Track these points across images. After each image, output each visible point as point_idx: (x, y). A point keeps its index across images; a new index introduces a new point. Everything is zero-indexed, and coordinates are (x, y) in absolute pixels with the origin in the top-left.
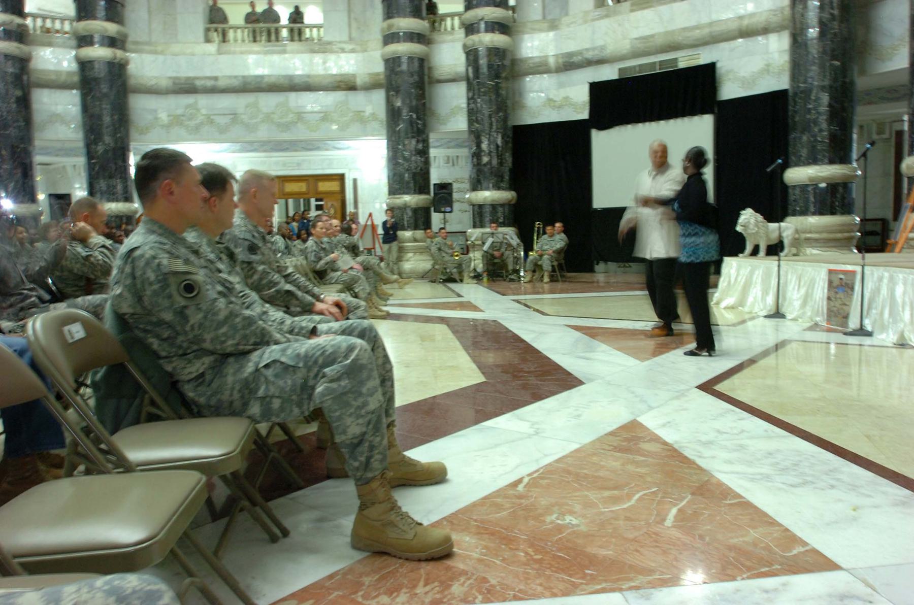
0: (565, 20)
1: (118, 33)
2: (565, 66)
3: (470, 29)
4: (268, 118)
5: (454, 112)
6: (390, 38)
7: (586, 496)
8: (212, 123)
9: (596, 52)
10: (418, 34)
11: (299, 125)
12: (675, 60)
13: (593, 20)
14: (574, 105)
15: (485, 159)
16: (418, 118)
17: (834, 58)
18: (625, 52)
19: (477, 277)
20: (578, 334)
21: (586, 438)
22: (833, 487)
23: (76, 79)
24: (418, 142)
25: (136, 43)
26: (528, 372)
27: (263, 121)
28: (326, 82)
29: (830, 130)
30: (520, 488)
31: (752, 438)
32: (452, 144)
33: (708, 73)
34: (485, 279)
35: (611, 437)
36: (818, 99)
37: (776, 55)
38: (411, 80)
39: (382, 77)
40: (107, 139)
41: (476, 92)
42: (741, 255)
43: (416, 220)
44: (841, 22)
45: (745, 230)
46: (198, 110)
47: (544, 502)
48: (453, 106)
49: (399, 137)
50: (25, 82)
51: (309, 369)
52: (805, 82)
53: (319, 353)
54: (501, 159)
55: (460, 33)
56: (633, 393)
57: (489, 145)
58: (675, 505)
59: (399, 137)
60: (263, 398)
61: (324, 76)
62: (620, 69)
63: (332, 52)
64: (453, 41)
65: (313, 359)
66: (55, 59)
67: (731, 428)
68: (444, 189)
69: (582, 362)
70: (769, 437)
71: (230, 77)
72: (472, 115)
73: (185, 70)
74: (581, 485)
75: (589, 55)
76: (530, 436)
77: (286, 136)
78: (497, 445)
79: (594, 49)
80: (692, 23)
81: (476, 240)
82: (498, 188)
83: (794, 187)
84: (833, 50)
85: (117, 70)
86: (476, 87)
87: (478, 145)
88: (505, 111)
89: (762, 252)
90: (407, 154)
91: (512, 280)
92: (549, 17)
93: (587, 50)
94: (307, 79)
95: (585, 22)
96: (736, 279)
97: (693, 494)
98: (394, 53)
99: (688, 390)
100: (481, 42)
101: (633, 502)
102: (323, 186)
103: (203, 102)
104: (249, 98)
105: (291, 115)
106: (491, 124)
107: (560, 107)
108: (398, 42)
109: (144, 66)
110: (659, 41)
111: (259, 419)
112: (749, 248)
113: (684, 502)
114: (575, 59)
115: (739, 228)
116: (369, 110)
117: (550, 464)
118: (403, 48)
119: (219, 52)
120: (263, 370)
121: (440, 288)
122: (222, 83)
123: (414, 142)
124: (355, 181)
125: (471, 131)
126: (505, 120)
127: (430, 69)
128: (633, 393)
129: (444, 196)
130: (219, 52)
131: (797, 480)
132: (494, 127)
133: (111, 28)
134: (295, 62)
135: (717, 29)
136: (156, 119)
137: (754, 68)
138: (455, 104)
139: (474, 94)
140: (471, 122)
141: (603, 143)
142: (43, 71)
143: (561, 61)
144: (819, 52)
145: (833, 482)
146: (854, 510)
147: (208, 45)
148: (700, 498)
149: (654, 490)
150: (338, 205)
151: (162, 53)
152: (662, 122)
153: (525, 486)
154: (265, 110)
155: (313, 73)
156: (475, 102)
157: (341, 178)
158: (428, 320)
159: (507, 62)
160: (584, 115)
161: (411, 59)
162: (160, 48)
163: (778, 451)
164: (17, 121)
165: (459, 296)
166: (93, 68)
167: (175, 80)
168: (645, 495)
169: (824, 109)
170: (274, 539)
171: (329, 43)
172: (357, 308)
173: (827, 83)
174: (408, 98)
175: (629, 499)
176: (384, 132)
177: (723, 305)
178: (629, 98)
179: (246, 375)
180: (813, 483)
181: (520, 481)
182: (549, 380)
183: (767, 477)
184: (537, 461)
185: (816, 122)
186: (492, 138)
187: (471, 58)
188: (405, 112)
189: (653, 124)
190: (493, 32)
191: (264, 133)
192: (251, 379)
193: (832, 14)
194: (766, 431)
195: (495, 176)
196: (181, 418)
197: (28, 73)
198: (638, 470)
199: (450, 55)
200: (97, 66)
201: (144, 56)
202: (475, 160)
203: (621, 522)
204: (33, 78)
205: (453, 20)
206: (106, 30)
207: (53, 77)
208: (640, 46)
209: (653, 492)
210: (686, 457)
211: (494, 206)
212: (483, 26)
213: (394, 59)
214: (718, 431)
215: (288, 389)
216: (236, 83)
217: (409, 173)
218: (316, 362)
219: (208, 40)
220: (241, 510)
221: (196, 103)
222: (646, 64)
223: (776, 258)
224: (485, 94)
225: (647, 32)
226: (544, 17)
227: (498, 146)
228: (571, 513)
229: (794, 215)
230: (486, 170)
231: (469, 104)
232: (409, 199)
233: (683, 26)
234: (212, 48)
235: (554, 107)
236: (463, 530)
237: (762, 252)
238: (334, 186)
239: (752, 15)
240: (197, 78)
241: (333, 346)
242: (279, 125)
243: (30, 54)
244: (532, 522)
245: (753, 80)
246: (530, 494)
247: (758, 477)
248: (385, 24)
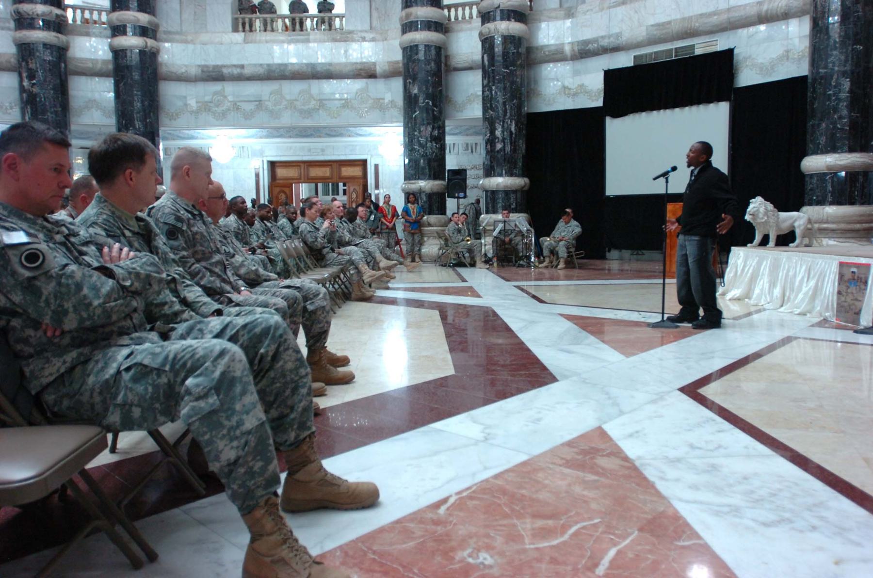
0: (581, 8)
1: (149, 22)
2: (581, 53)
3: (486, 17)
4: (291, 105)
5: (469, 101)
6: (408, 27)
7: (514, 526)
8: (238, 109)
9: (612, 39)
10: (436, 23)
11: (321, 111)
12: (692, 47)
13: (610, 7)
14: (588, 93)
15: (499, 146)
16: (434, 105)
17: (857, 42)
18: (640, 39)
19: (488, 261)
20: (568, 324)
21: (540, 447)
22: (814, 528)
23: (111, 67)
24: (433, 128)
25: (169, 33)
26: (503, 366)
27: (286, 108)
28: (346, 70)
29: (850, 117)
30: (442, 510)
31: (727, 456)
32: (471, 131)
33: (725, 60)
34: (495, 264)
35: (566, 449)
36: (838, 85)
37: (796, 41)
39: (401, 65)
41: (491, 79)
42: (749, 245)
43: (430, 207)
45: (754, 219)
46: (225, 97)
47: (462, 531)
48: (469, 91)
49: (415, 124)
50: (63, 70)
51: (177, 374)
52: (826, 67)
53: (188, 356)
54: (515, 146)
55: (477, 22)
56: (607, 394)
57: (503, 132)
58: (615, 545)
60: (123, 405)
61: (346, 64)
62: (635, 57)
63: (353, 40)
64: (471, 30)
65: (181, 362)
66: (93, 48)
67: (706, 442)
68: (459, 175)
69: (563, 356)
70: (748, 456)
71: (255, 65)
72: (488, 103)
73: (213, 58)
74: (513, 510)
75: (605, 43)
76: (477, 443)
77: (308, 122)
78: (436, 453)
79: (609, 37)
80: (711, 9)
81: (487, 225)
82: (511, 175)
83: (811, 176)
84: (856, 34)
85: (149, 58)
86: (491, 75)
87: (492, 132)
88: (520, 99)
89: (772, 243)
90: (422, 140)
91: (522, 266)
92: (566, 5)
93: (603, 37)
94: (328, 67)
95: (602, 9)
96: (743, 270)
97: (641, 530)
98: (412, 41)
99: (669, 392)
100: (496, 29)
101: (566, 537)
102: (347, 172)
103: (229, 88)
104: (273, 86)
105: (313, 102)
106: (505, 112)
107: (575, 95)
108: (417, 30)
109: (174, 54)
110: (675, 28)
111: (119, 428)
112: (758, 238)
113: (627, 541)
114: (591, 47)
115: (747, 217)
116: (388, 97)
117: (487, 480)
118: (420, 36)
119: (246, 41)
120: (123, 373)
121: (450, 271)
122: (247, 71)
123: (429, 129)
124: (376, 166)
125: (485, 118)
126: (520, 107)
127: (447, 57)
128: (607, 394)
129: (457, 181)
130: (246, 41)
131: (772, 517)
132: (508, 114)
133: (144, 18)
134: (318, 51)
135: (736, 14)
136: (186, 105)
137: (773, 53)
138: (471, 91)
139: (489, 82)
140: (485, 110)
141: (619, 132)
142: (82, 60)
143: (576, 48)
144: (840, 36)
145: (816, 522)
146: (837, 563)
147: (236, 34)
148: (648, 536)
149: (596, 521)
150: (360, 189)
151: (192, 42)
152: (677, 110)
153: (448, 509)
154: (288, 97)
155: (335, 61)
156: (491, 90)
157: (364, 163)
158: (419, 304)
159: (522, 50)
160: (599, 103)
161: (427, 47)
162: (189, 38)
163: (756, 474)
164: (55, 106)
165: (464, 280)
166: (126, 56)
167: (204, 68)
168: (584, 528)
169: (843, 95)
170: (136, 565)
171: (351, 32)
172: (316, 295)
173: (848, 68)
175: (563, 533)
176: (402, 119)
177: (729, 296)
178: (644, 86)
179: (107, 376)
180: (790, 521)
181: (445, 501)
182: (521, 375)
183: (735, 511)
184: (474, 475)
185: (836, 110)
186: (506, 125)
187: (487, 46)
188: (421, 100)
189: (668, 111)
190: (509, 20)
191: (287, 119)
192: (112, 382)
194: (746, 447)
195: (508, 162)
196: (31, 424)
197: (65, 62)
198: (585, 493)
199: (467, 45)
200: (129, 54)
201: (175, 45)
202: (489, 147)
203: (543, 566)
204: (71, 67)
205: (471, 9)
206: (138, 20)
207: (90, 65)
208: (657, 33)
209: (594, 525)
210: (645, 479)
211: (507, 193)
212: (498, 12)
213: (411, 47)
214: (692, 446)
215: (148, 397)
216: (261, 71)
217: (426, 158)
218: (185, 364)
219: (235, 30)
220: (97, 530)
221: (223, 89)
222: (663, 51)
223: (656, 255)
224: (500, 81)
225: (662, 19)
226: (561, 5)
227: (511, 132)
228: (488, 548)
229: (810, 204)
230: (499, 156)
231: (483, 92)
232: (424, 185)
233: (700, 12)
234: (239, 37)
235: (569, 95)
236: (355, 565)
237: (772, 243)
238: (356, 171)
240: (225, 66)
241: (206, 348)
242: (301, 112)
243: (68, 42)
244: (438, 558)
245: (773, 66)
246: (451, 519)
247: (726, 509)
248: (404, 13)
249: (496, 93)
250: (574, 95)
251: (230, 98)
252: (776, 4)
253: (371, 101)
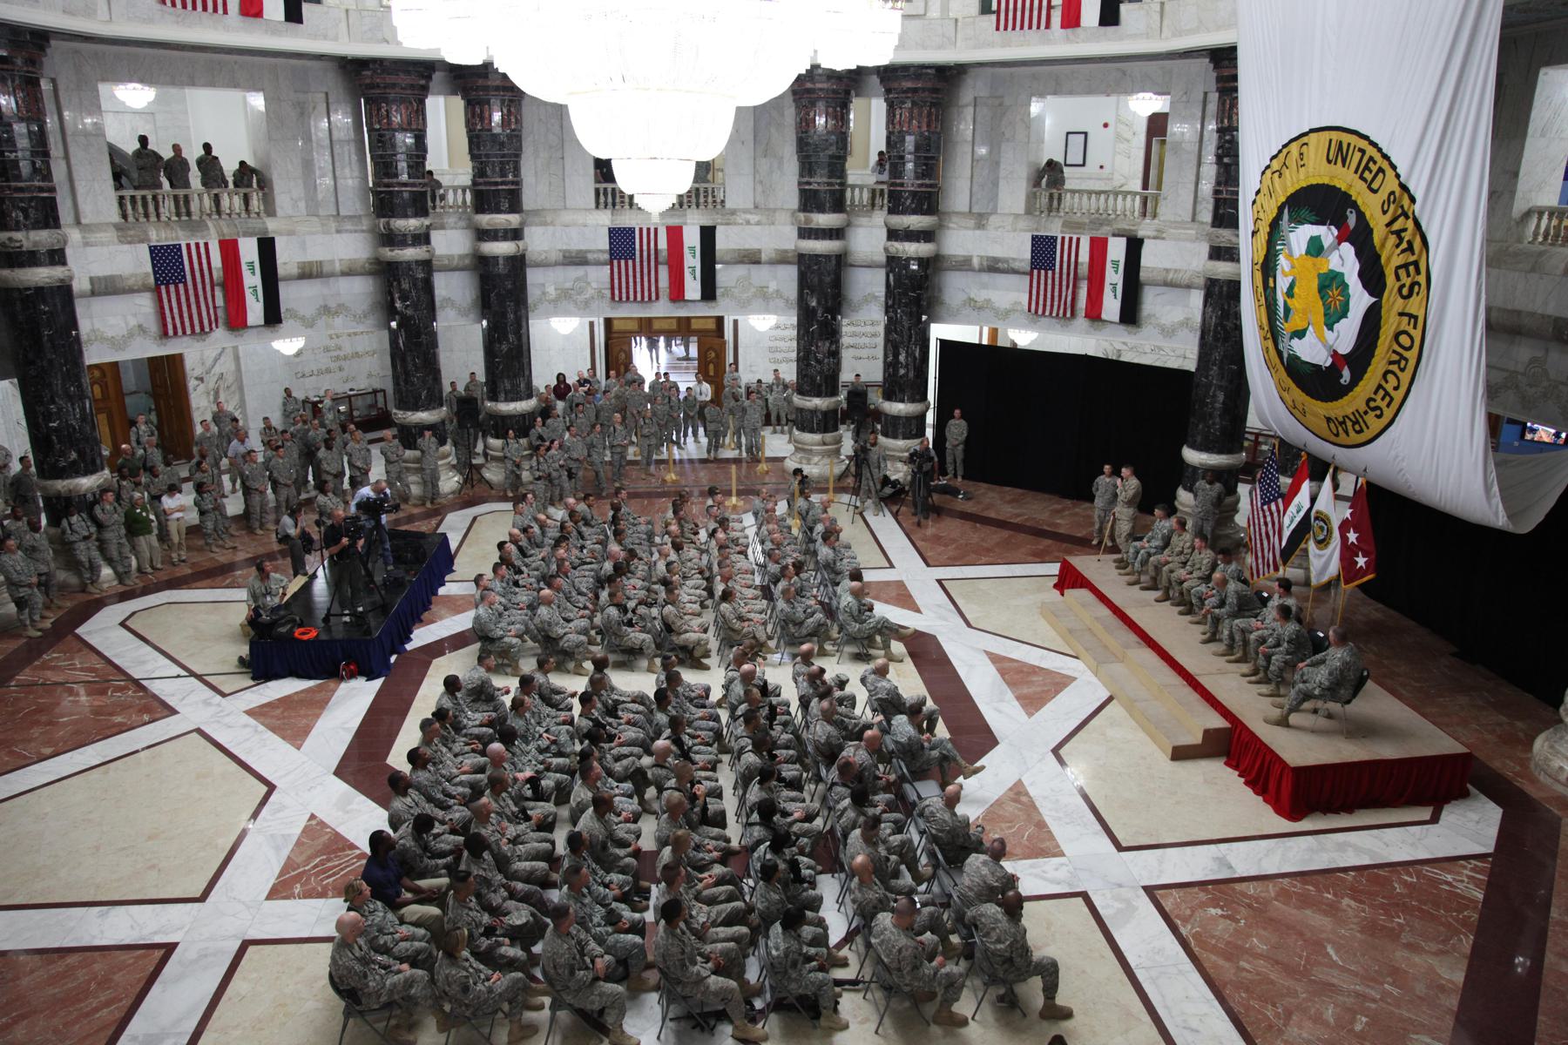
3: (893, 235)
15: (902, 372)
36: (1214, 396)
38: (828, 279)
40: (511, 337)
87: (896, 355)
90: (819, 356)
114: (1000, 265)
116: (773, 286)
124: (736, 322)
136: (544, 293)
151: (552, 224)
161: (827, 257)
169: (1218, 405)
171: (733, 212)
174: (821, 293)
185: (1211, 415)
248: (802, 216)
251: (594, 285)
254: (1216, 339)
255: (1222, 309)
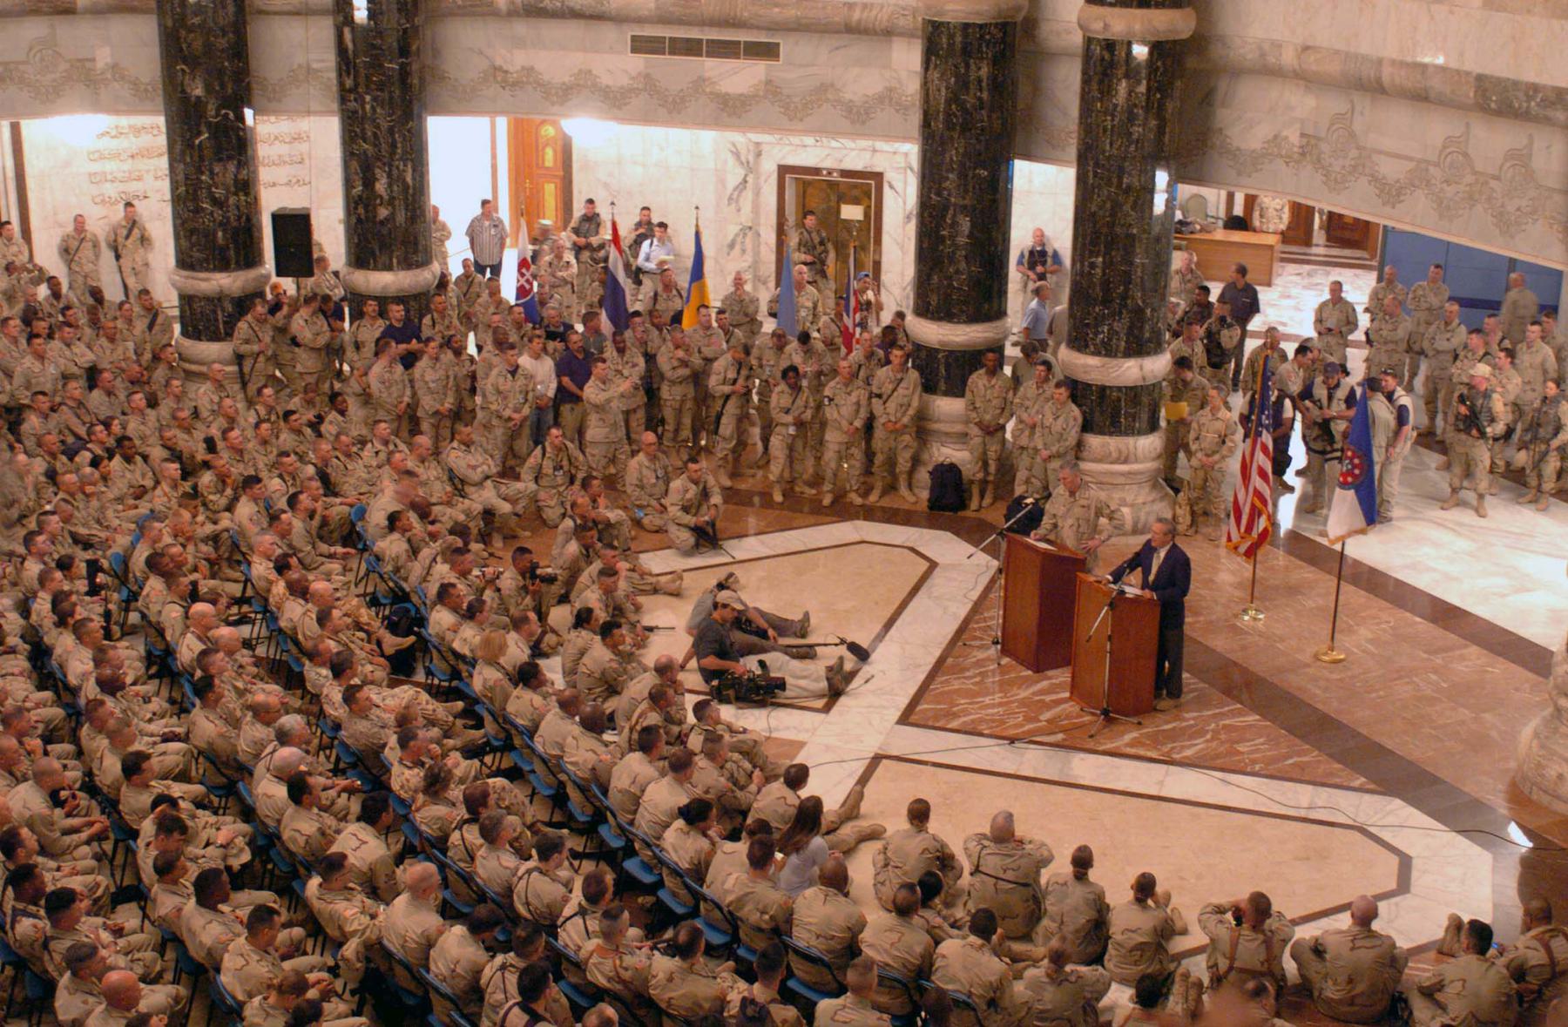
36: (954, 224)
44: (992, 110)
49: (202, 159)
52: (939, 194)
57: (390, 185)
59: (202, 159)
62: (633, 37)
87: (369, 183)
90: (219, 192)
116: (104, 57)
169: (962, 240)
185: (952, 259)
186: (395, 172)
188: (211, 109)
193: (980, 99)
239: (865, 6)
249: (373, 108)
250: (514, 84)
252: (874, 12)
253: (63, 66)
254: (949, 126)
255: (957, 76)
